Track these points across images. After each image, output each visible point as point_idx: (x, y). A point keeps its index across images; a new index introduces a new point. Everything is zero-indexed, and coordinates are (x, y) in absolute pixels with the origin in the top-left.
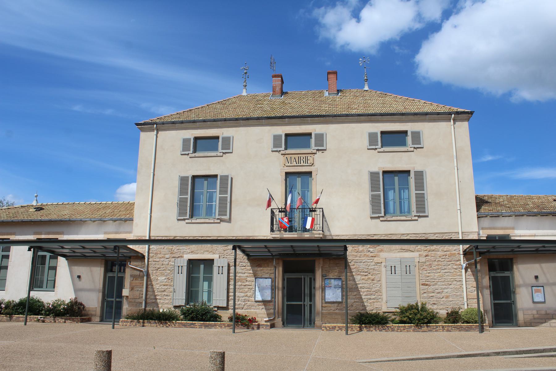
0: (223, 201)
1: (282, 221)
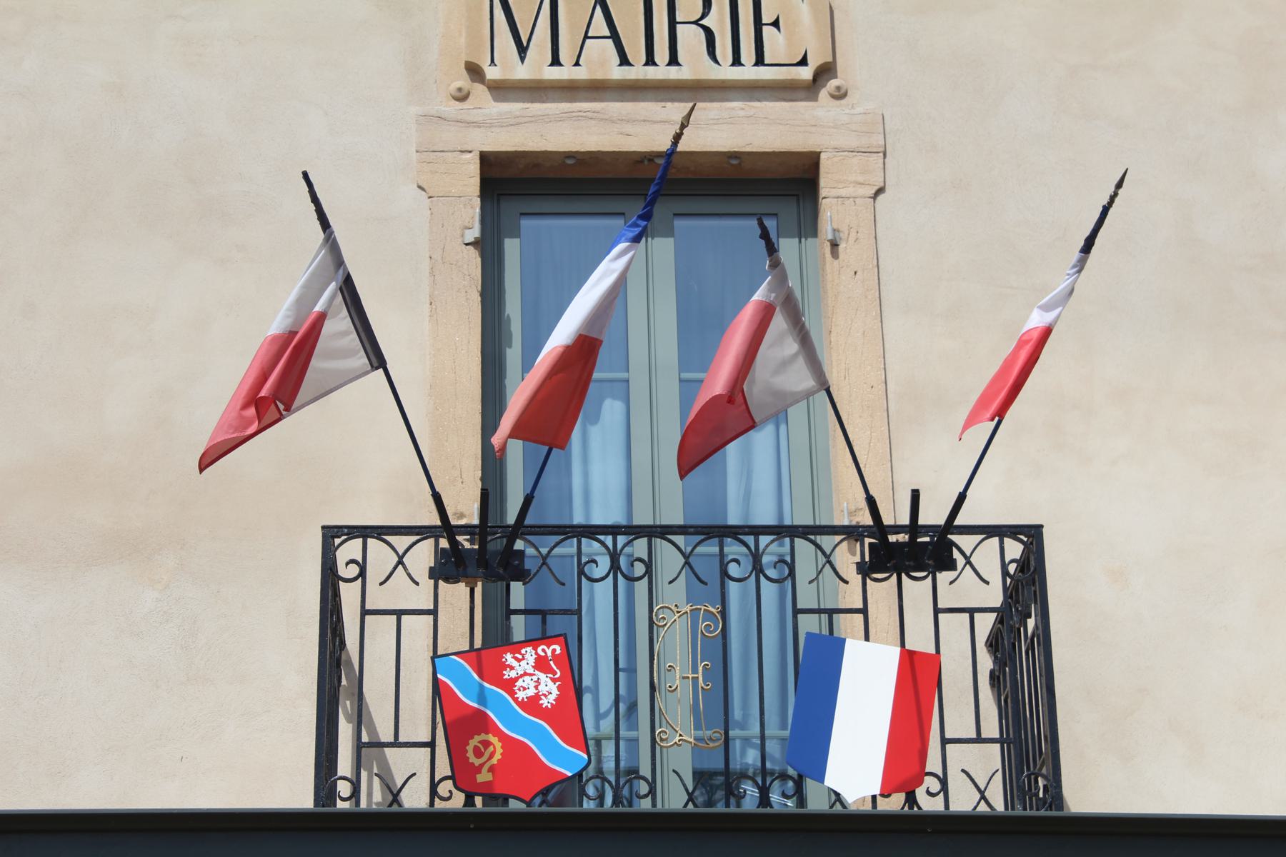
1: (482, 698)
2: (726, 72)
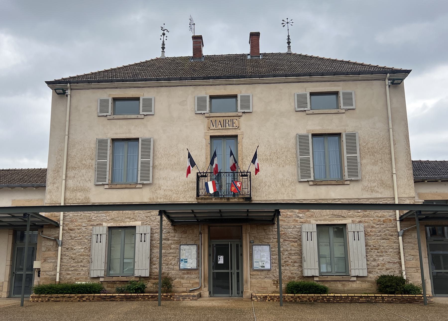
0: (146, 166)
2: (230, 128)
